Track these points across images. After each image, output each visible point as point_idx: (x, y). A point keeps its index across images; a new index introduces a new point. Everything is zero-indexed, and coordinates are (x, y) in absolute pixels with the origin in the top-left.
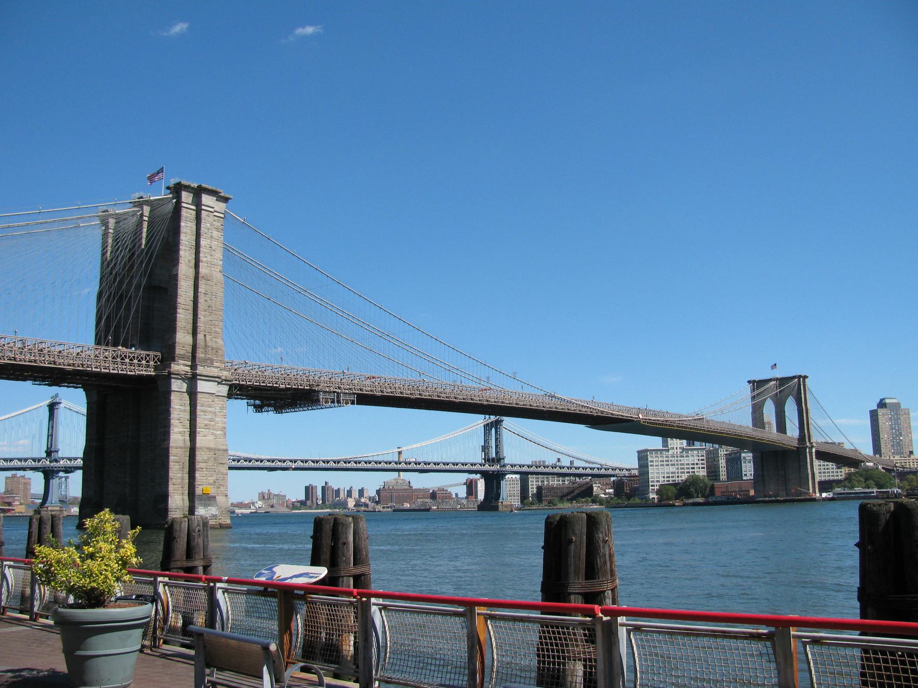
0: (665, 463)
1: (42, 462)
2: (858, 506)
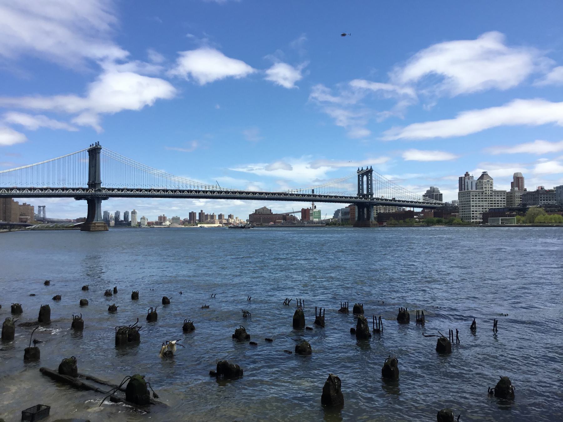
0: (481, 200)
1: (90, 191)
2: (23, 315)
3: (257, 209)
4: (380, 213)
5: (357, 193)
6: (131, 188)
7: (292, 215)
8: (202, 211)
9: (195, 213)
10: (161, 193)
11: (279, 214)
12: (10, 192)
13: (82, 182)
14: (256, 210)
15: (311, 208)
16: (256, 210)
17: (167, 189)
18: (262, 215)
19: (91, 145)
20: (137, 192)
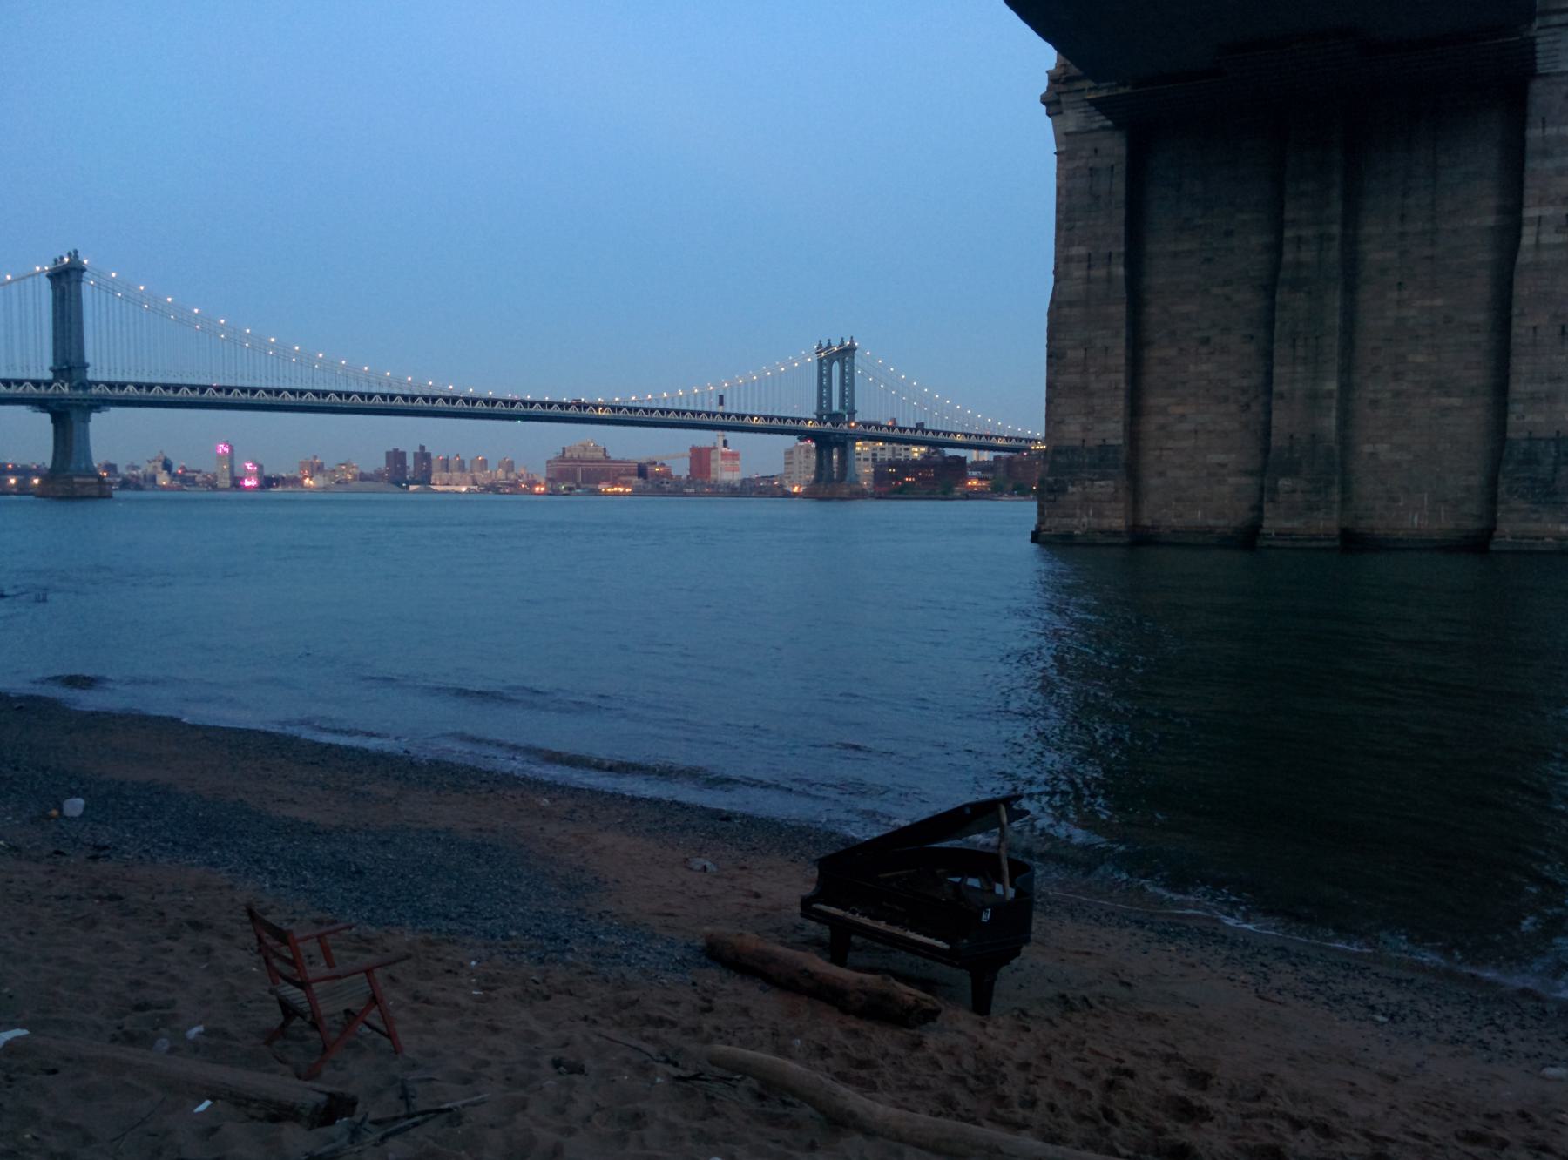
1: (55, 388)
4: (883, 460)
5: (815, 408)
6: (276, 386)
8: (422, 448)
9: (404, 454)
10: (286, 398)
12: (583, 411)
13: (38, 362)
14: (564, 449)
17: (327, 389)
18: (582, 461)
19: (56, 261)
20: (243, 396)
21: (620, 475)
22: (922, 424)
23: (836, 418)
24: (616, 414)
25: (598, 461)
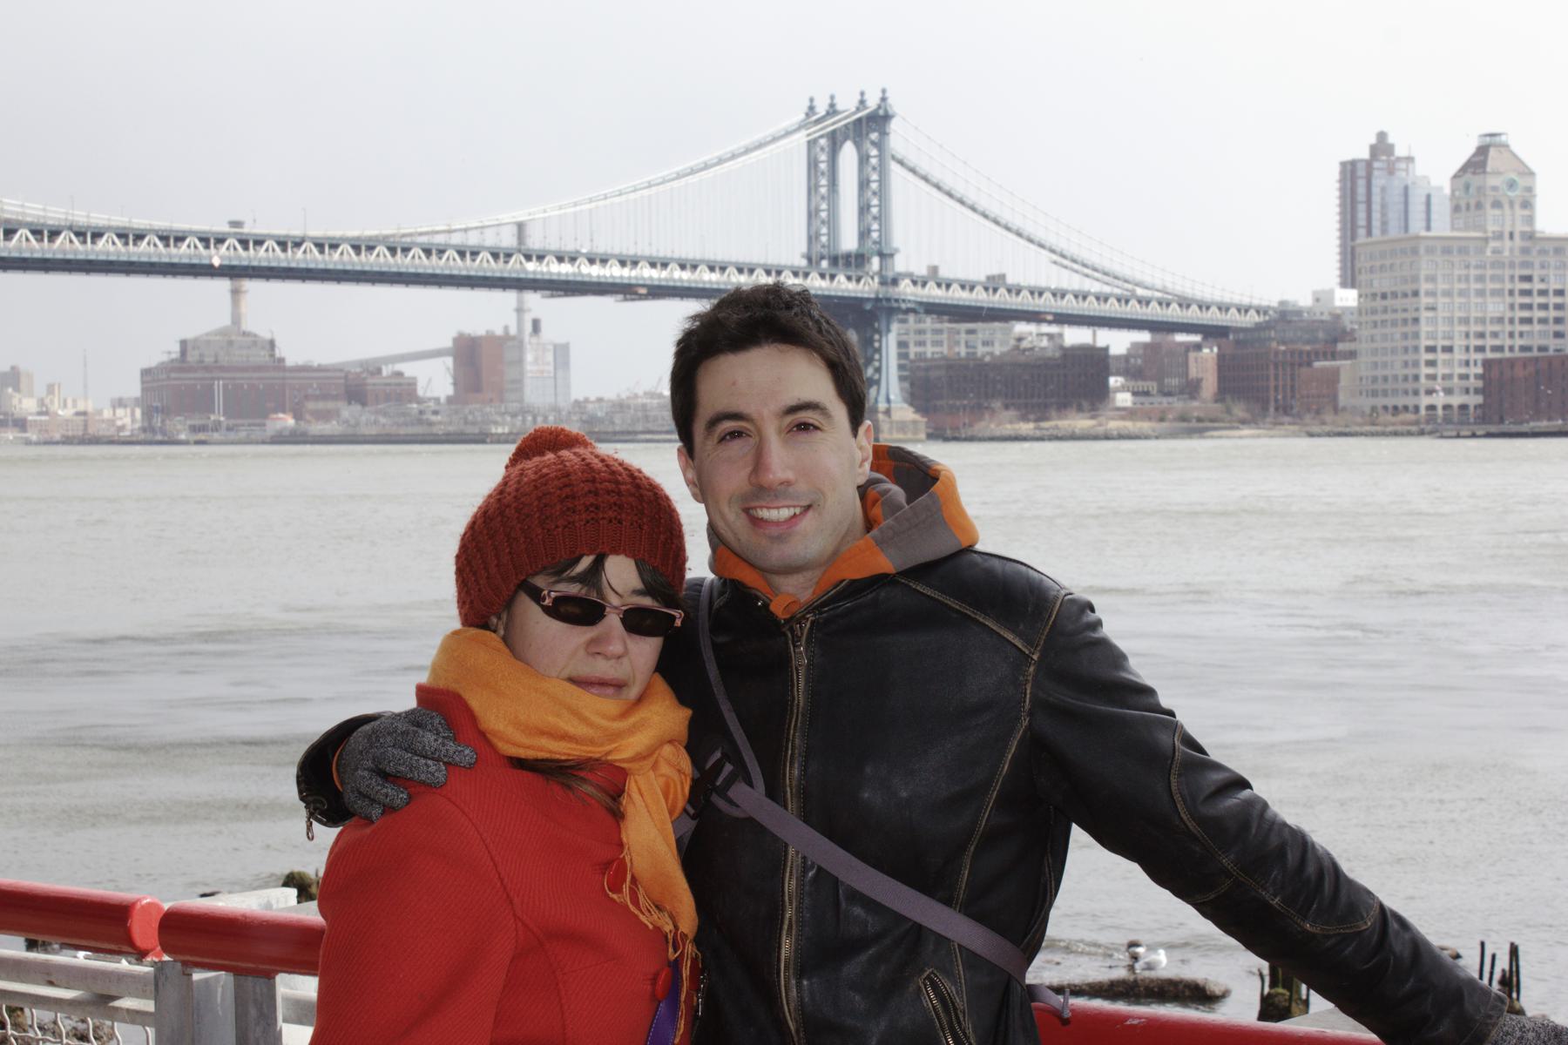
3: (189, 335)
4: (921, 357)
7: (399, 374)
11: (320, 369)
14: (184, 343)
15: (506, 328)
16: (184, 343)
18: (222, 369)
21: (307, 397)
22: (1003, 277)
23: (854, 262)
24: (173, 250)
25: (259, 368)
